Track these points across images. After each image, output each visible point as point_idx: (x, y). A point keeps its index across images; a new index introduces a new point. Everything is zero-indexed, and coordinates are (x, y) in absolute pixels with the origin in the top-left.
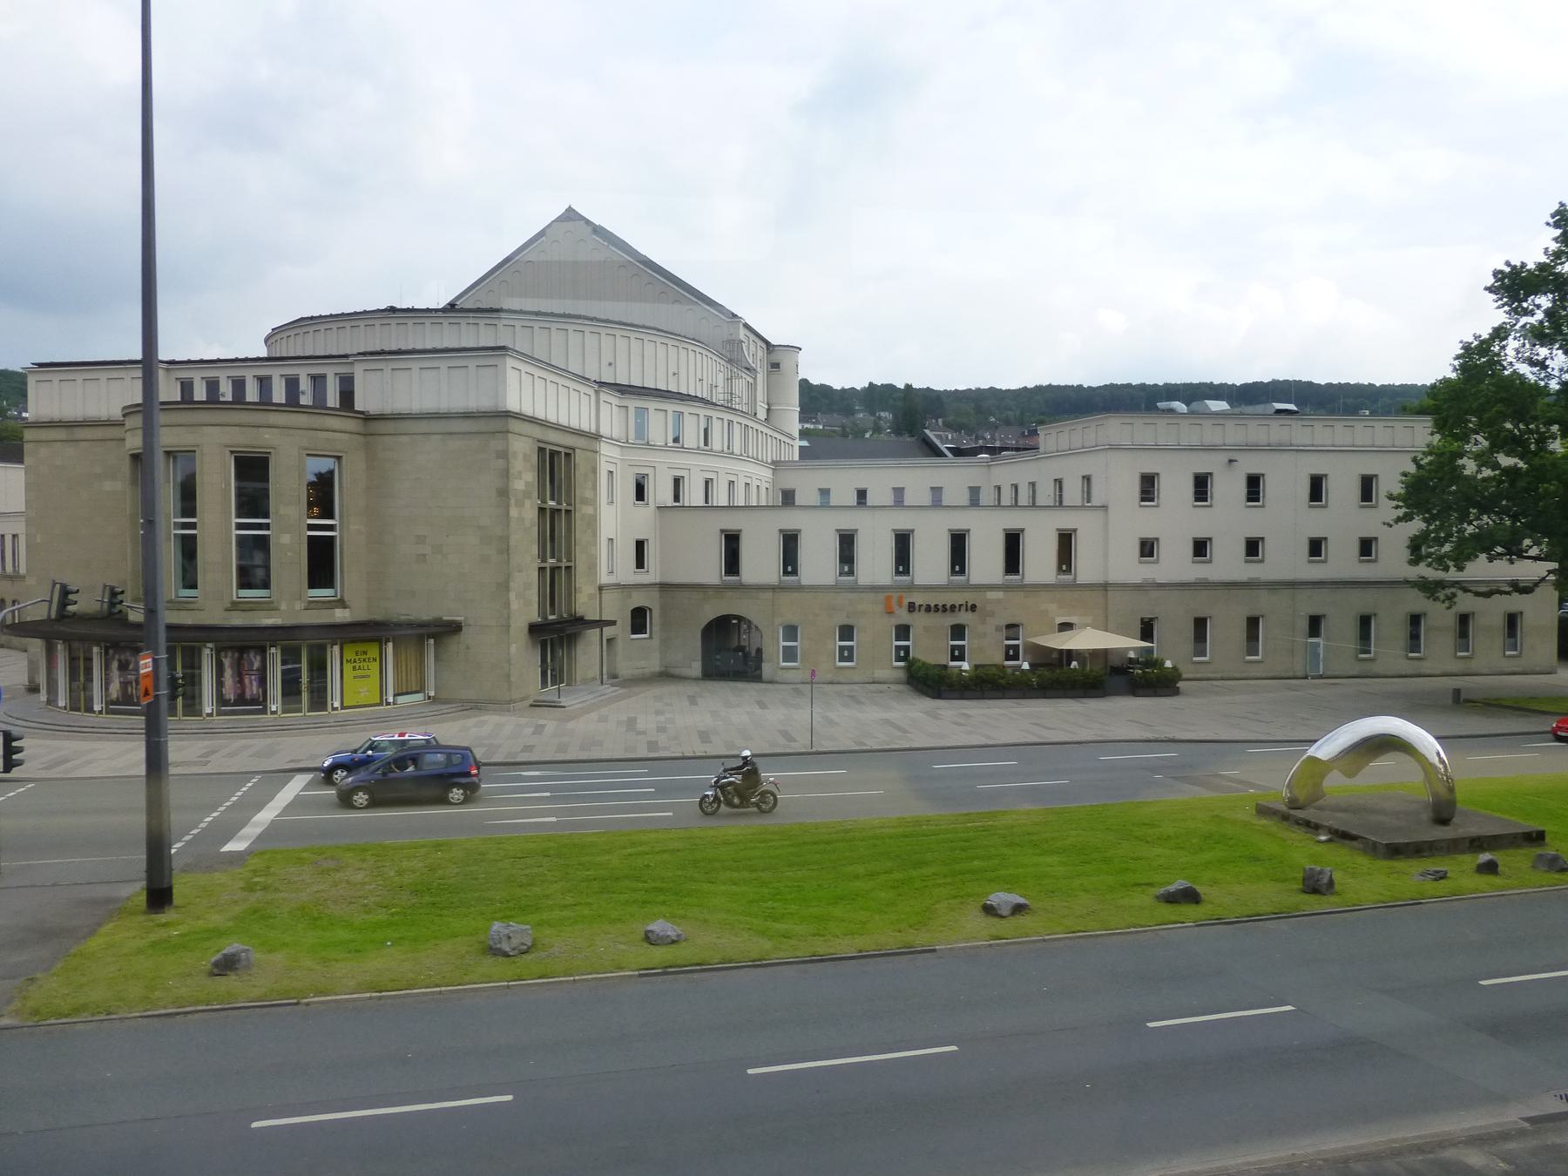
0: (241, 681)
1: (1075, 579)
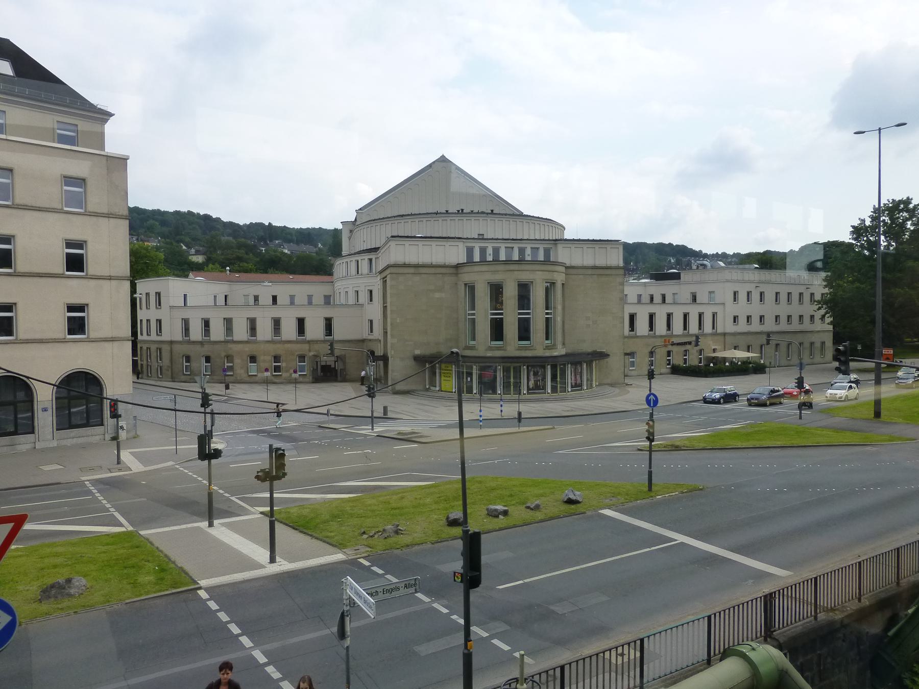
0: (576, 378)
1: (655, 334)
